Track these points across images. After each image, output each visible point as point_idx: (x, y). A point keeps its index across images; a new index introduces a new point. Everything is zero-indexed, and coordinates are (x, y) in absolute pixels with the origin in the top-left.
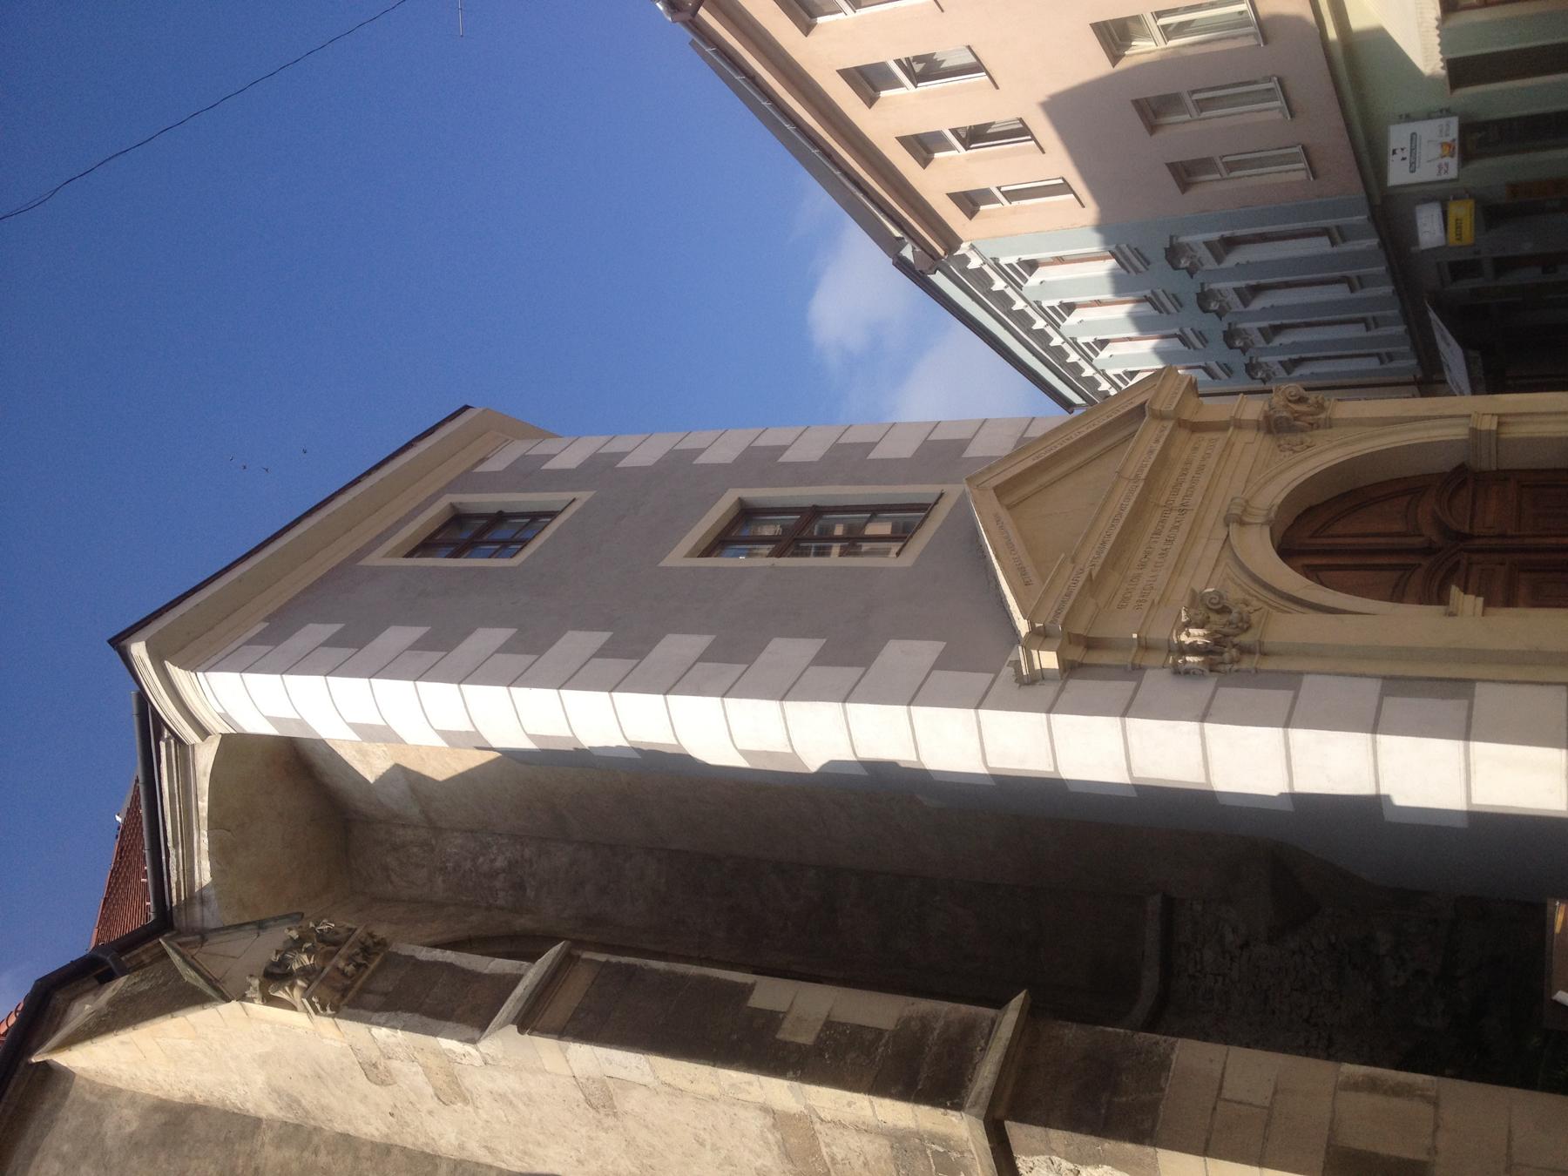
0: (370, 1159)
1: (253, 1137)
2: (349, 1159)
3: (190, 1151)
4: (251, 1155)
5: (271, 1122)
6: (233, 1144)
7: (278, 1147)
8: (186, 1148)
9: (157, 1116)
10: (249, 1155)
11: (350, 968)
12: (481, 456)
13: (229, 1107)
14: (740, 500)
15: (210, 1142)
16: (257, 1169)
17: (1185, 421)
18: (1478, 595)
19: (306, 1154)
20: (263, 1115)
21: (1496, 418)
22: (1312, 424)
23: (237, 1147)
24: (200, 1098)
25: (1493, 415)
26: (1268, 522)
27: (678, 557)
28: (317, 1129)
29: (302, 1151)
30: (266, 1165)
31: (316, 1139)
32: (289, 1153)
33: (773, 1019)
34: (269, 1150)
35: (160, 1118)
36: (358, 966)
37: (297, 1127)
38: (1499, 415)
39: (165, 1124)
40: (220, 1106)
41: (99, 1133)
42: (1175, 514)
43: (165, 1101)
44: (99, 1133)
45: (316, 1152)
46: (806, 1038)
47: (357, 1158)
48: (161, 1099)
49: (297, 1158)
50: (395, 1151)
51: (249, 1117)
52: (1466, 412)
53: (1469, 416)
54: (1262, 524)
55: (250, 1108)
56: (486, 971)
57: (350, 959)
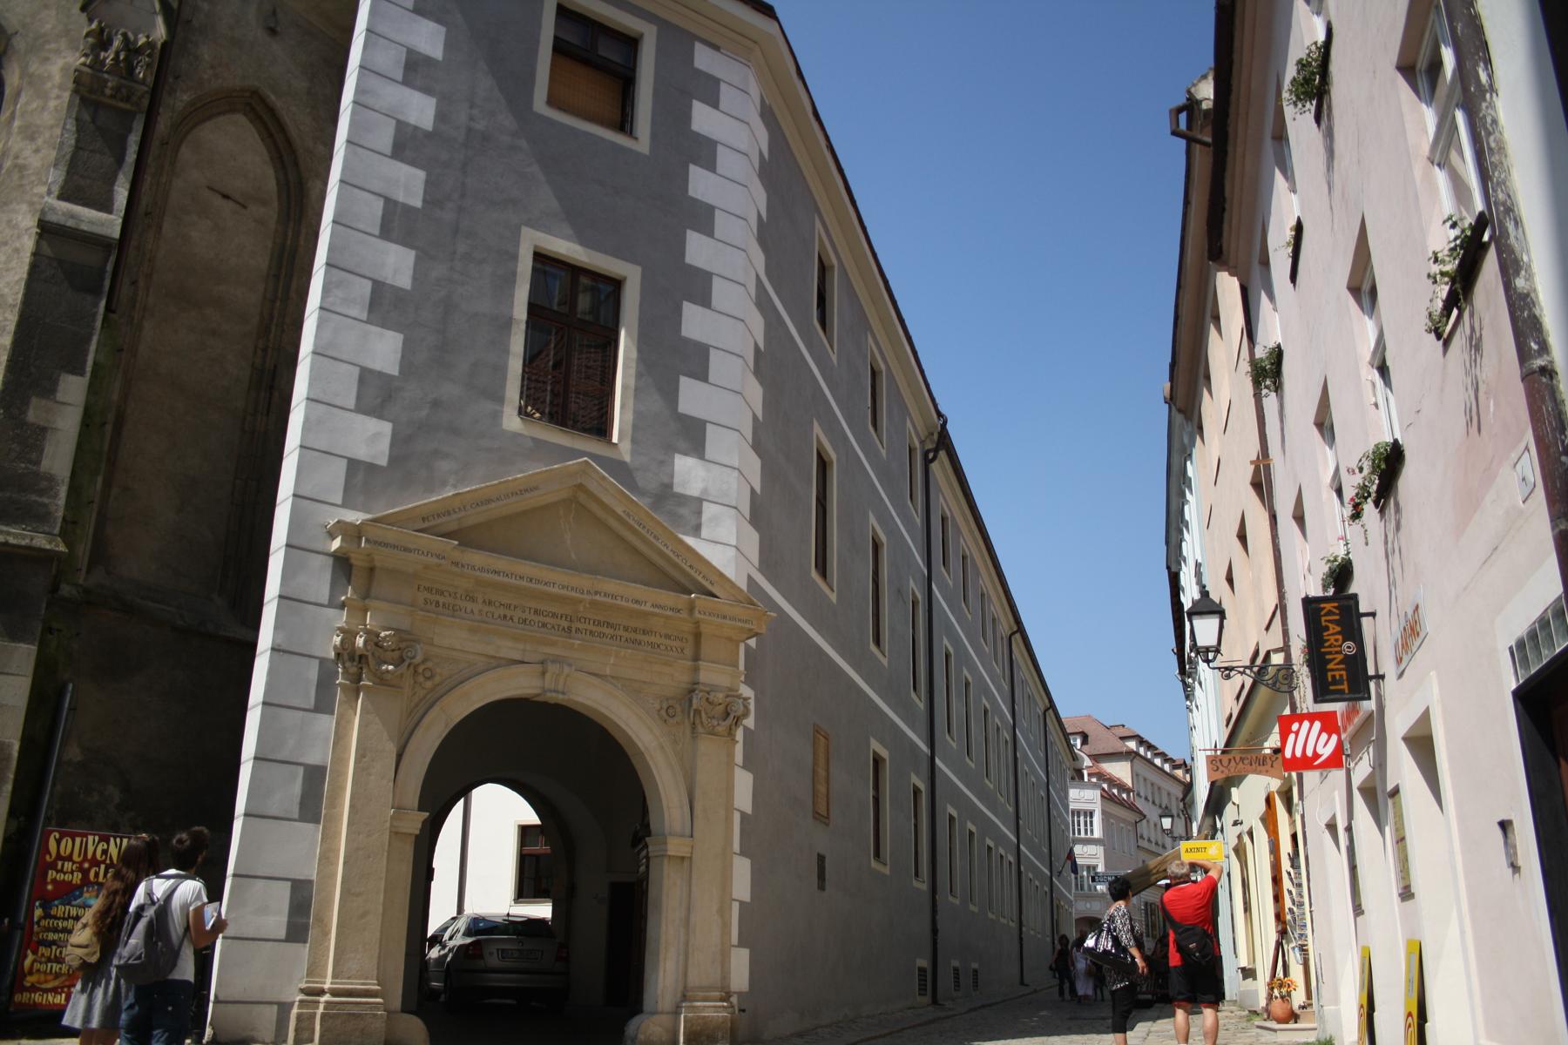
0: (51, 136)
4: (58, 52)
11: (108, 92)
12: (718, 43)
14: (625, 279)
17: (699, 627)
18: (421, 830)
21: (689, 855)
22: (694, 724)
25: (692, 853)
26: (545, 691)
27: (531, 240)
33: (49, 391)
36: (112, 97)
38: (691, 858)
42: (565, 624)
45: (58, 97)
46: (32, 416)
52: (695, 834)
53: (692, 836)
54: (543, 688)
56: (116, 188)
57: (117, 89)
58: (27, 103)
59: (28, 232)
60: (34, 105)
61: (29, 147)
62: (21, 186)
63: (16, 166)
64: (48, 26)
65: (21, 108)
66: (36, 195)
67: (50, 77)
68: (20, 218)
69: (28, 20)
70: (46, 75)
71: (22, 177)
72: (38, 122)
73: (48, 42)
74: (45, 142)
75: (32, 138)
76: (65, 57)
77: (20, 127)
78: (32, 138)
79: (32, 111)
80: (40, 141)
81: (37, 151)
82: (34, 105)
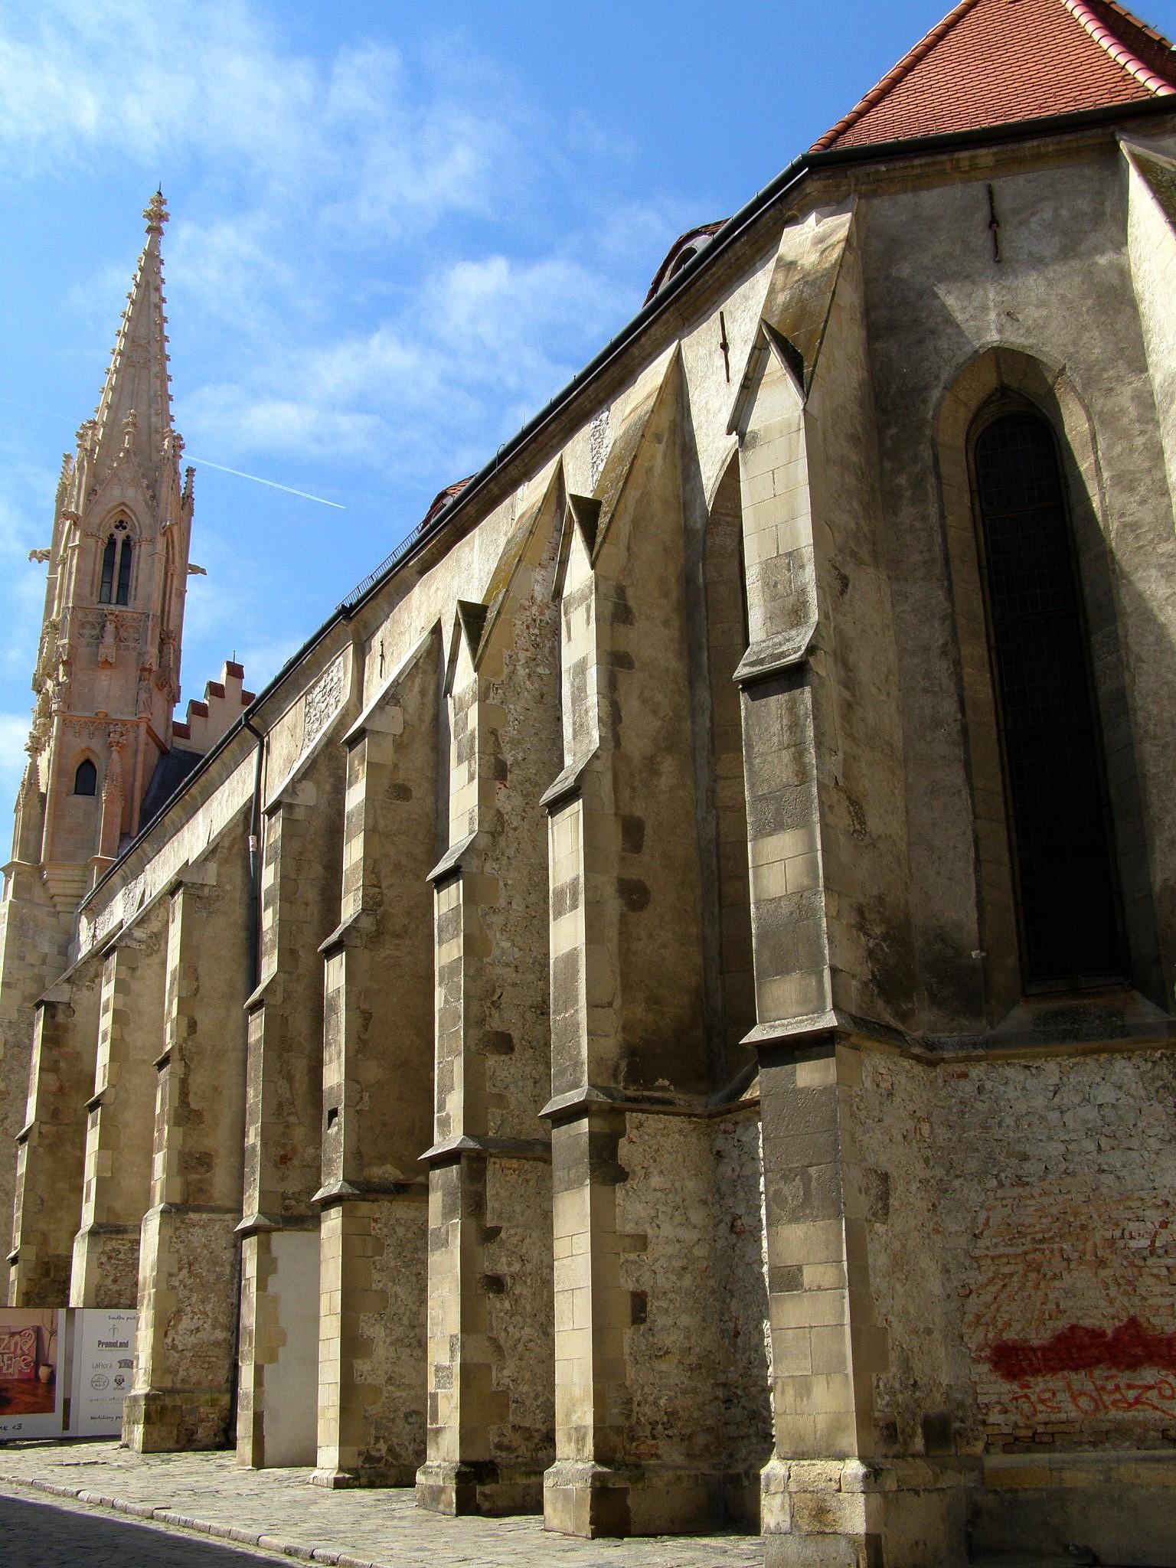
1: (1134, 371)
2: (1147, 465)
3: (1103, 322)
4: (1119, 379)
5: (1148, 381)
6: (1122, 358)
7: (1133, 398)
8: (1103, 319)
9: (1116, 276)
10: (1119, 376)
13: (1146, 338)
15: (1115, 336)
16: (1111, 389)
19: (1137, 425)
20: (1151, 371)
23: (1121, 362)
24: (1143, 308)
28: (1157, 424)
29: (1138, 421)
30: (1117, 395)
31: (1150, 427)
32: (1132, 411)
34: (1128, 391)
35: (1115, 280)
37: (1153, 406)
39: (1113, 287)
40: (1144, 328)
41: (1086, 233)
43: (1130, 276)
44: (1086, 233)
45: (1142, 432)
47: (1150, 470)
48: (1130, 271)
49: (1131, 420)
50: (1166, 500)
51: (1145, 360)
55: (1152, 359)
58: (1110, 447)
59: (1170, 601)
60: (1119, 449)
61: (1132, 499)
62: (1140, 547)
63: (1125, 525)
64: (1097, 351)
65: (1103, 454)
66: (1162, 555)
67: (1123, 411)
68: (1153, 587)
69: (1071, 349)
70: (1116, 409)
71: (1137, 537)
72: (1132, 467)
73: (1104, 369)
74: (1149, 490)
75: (1132, 490)
76: (1130, 383)
77: (1112, 478)
78: (1132, 490)
79: (1118, 456)
80: (1142, 490)
81: (1143, 502)
82: (1119, 449)
